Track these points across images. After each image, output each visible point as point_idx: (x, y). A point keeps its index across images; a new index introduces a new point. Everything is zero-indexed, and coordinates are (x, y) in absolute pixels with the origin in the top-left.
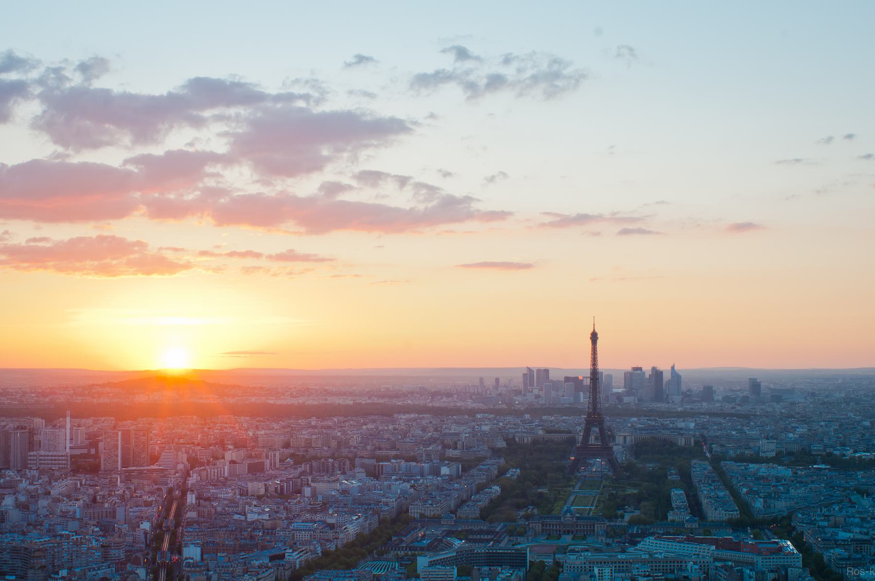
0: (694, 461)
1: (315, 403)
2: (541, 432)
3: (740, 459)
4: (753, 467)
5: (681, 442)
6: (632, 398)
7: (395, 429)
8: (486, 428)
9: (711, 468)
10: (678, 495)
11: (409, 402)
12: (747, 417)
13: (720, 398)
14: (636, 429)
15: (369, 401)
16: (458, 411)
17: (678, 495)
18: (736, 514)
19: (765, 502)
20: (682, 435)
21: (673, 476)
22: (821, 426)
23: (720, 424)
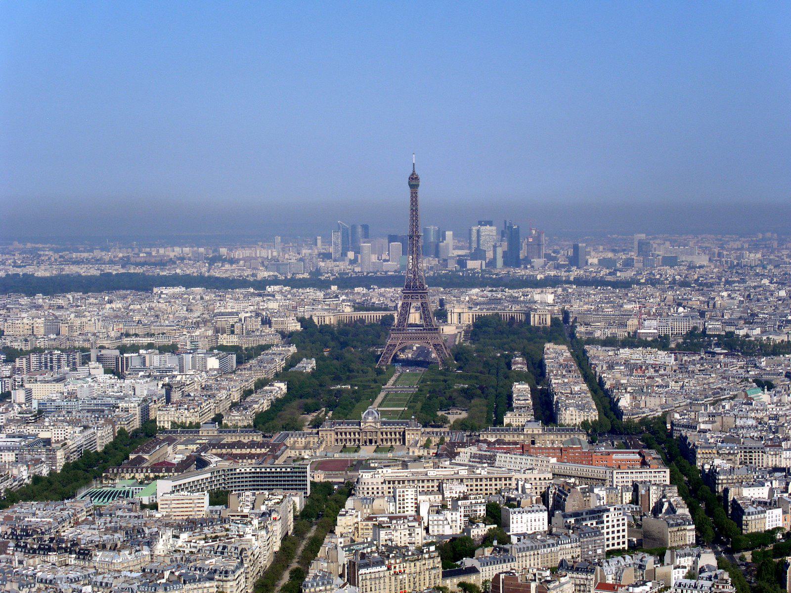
0: (547, 345)
1: (48, 274)
2: (348, 310)
3: (610, 342)
4: (625, 353)
5: (535, 320)
6: (480, 261)
7: (150, 309)
8: (273, 305)
9: (569, 354)
10: (521, 390)
11: (178, 271)
12: (626, 285)
13: (595, 261)
14: (477, 304)
15: (122, 271)
16: (243, 283)
17: (521, 390)
18: (593, 415)
19: (634, 398)
20: (536, 310)
21: (519, 364)
22: (722, 297)
23: (589, 295)
